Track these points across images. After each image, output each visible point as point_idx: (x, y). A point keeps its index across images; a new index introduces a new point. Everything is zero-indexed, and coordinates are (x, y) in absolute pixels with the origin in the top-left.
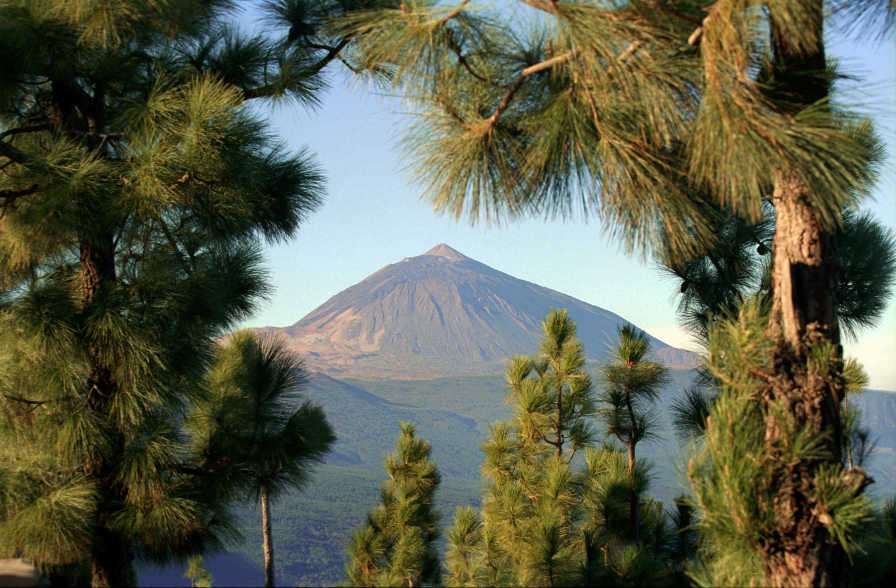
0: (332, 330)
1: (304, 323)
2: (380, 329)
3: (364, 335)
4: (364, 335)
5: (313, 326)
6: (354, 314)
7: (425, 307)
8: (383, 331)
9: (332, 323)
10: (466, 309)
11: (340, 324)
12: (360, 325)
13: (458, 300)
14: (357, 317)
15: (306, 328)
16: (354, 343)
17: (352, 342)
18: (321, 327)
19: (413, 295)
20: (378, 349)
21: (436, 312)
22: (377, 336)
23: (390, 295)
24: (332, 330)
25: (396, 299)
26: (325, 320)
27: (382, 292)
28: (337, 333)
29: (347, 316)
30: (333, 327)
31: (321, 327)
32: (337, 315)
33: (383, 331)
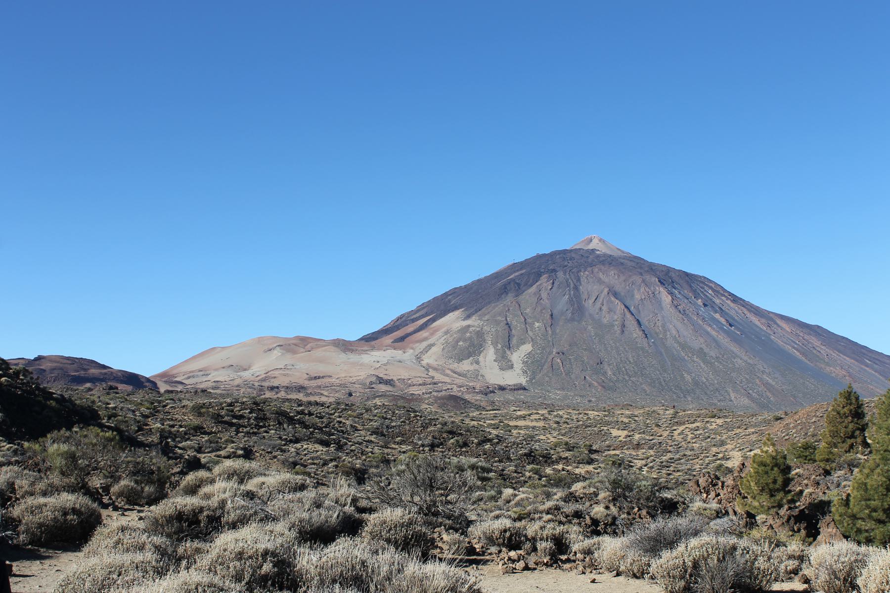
0: (424, 344)
1: (370, 339)
2: (522, 342)
3: (489, 355)
4: (489, 355)
5: (388, 340)
6: (468, 317)
7: (604, 308)
8: (527, 348)
9: (424, 334)
10: (684, 313)
11: (440, 333)
12: (480, 334)
13: (666, 299)
14: (474, 322)
15: (373, 343)
16: (472, 368)
17: (466, 366)
18: (402, 339)
19: (576, 288)
20: (523, 381)
21: (628, 315)
22: (517, 357)
23: (533, 289)
24: (424, 344)
25: (544, 295)
26: (410, 328)
28: (434, 349)
29: (453, 321)
30: (426, 339)
31: (402, 339)
32: (433, 320)
33: (527, 348)
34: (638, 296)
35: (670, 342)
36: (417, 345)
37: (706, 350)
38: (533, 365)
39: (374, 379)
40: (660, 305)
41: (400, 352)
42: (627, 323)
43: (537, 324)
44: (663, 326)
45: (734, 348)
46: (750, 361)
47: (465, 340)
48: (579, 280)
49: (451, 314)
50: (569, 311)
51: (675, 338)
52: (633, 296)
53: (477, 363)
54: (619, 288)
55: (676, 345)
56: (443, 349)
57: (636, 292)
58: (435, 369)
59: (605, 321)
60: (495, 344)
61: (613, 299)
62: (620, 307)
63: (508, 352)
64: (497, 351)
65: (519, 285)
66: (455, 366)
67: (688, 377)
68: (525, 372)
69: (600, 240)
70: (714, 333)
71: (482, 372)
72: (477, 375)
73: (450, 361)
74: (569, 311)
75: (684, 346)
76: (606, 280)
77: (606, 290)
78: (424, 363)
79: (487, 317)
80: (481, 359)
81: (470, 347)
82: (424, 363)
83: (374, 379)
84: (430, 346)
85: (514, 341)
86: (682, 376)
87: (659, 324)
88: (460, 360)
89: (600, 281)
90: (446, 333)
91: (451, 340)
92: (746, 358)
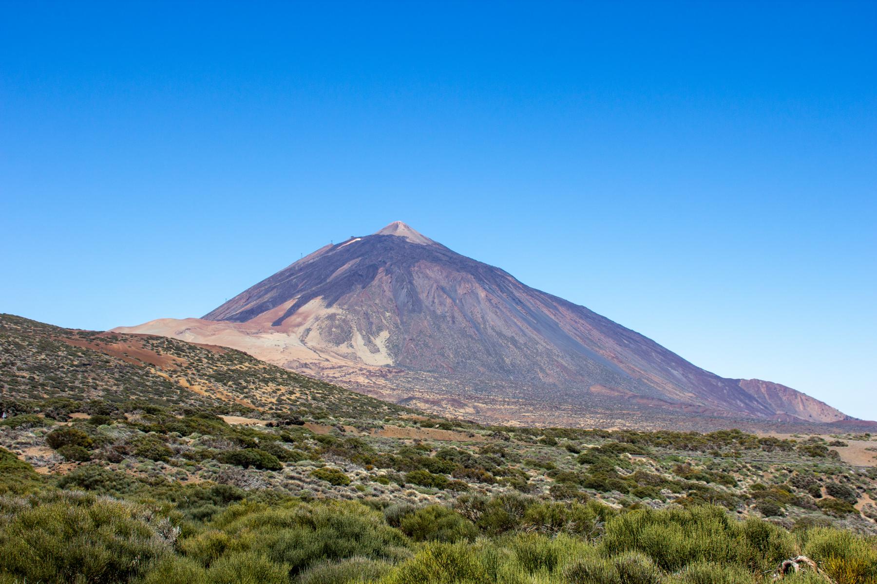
0: (301, 329)
2: (380, 329)
3: (358, 340)
4: (358, 340)
6: (329, 305)
7: (436, 301)
8: (385, 334)
9: (295, 319)
11: (311, 320)
16: (350, 350)
17: (343, 348)
19: (411, 283)
20: (390, 362)
22: (381, 340)
23: (375, 282)
24: (301, 329)
27: (362, 277)
28: (312, 334)
29: (315, 306)
30: (299, 325)
31: (278, 323)
32: (297, 306)
34: (461, 291)
35: (490, 331)
36: (296, 329)
37: (517, 338)
38: (394, 348)
39: (298, 364)
40: (478, 298)
41: (285, 335)
42: (456, 315)
43: (388, 314)
44: (483, 317)
45: (534, 335)
46: (548, 347)
47: (336, 327)
48: (411, 275)
49: (312, 302)
50: (410, 303)
51: (493, 329)
52: (456, 291)
53: (352, 346)
54: (443, 283)
55: (494, 334)
56: (320, 334)
57: (458, 287)
58: (321, 351)
59: (439, 312)
60: (360, 330)
61: (441, 293)
62: (449, 301)
63: (372, 338)
64: (363, 337)
65: (361, 276)
66: (336, 348)
67: (508, 361)
68: (389, 355)
69: (405, 226)
70: (519, 324)
71: (359, 354)
72: (355, 358)
73: (331, 345)
74: (410, 303)
75: (500, 334)
76: (433, 276)
77: (435, 285)
78: (310, 344)
79: (346, 307)
80: (353, 343)
81: (342, 335)
82: (310, 344)
83: (298, 364)
84: (308, 330)
85: (374, 328)
86: (503, 359)
87: (479, 316)
88: (338, 344)
89: (427, 277)
90: (317, 319)
91: (324, 326)
92: (545, 344)
